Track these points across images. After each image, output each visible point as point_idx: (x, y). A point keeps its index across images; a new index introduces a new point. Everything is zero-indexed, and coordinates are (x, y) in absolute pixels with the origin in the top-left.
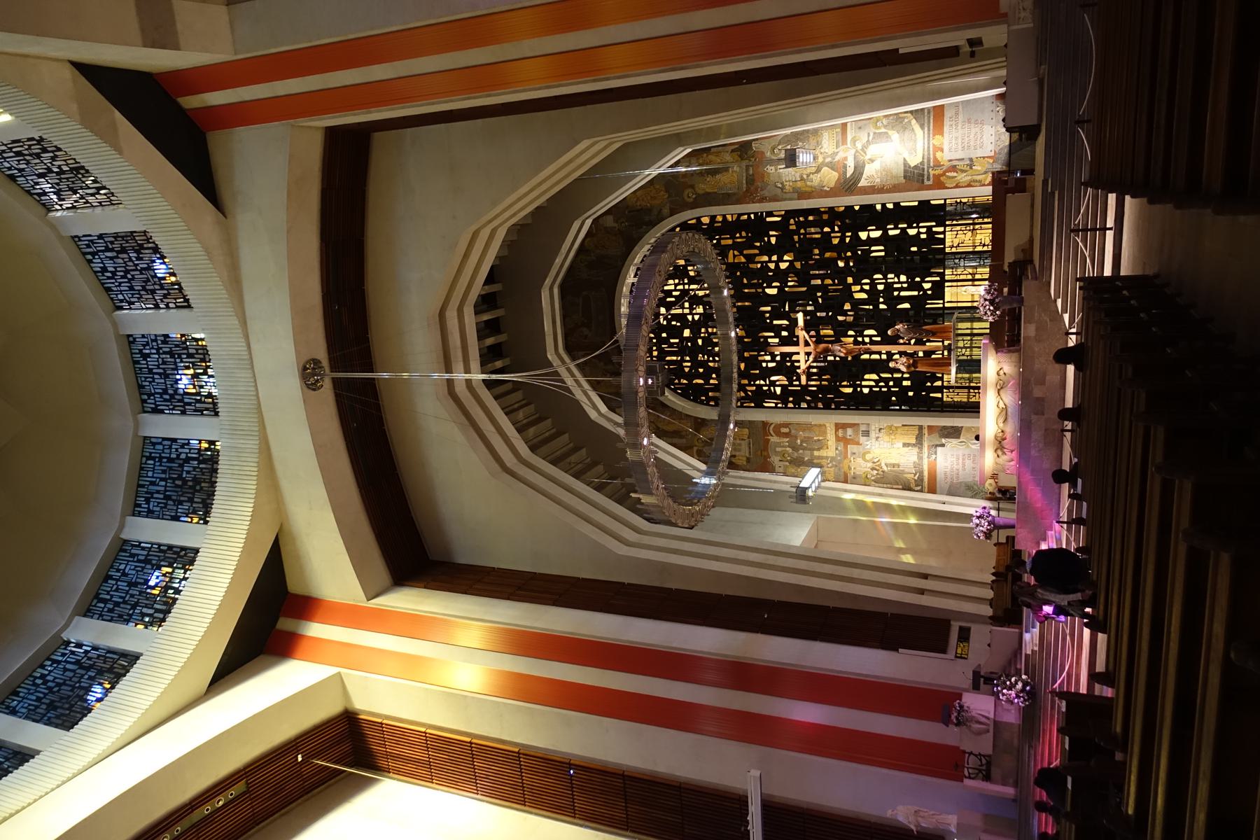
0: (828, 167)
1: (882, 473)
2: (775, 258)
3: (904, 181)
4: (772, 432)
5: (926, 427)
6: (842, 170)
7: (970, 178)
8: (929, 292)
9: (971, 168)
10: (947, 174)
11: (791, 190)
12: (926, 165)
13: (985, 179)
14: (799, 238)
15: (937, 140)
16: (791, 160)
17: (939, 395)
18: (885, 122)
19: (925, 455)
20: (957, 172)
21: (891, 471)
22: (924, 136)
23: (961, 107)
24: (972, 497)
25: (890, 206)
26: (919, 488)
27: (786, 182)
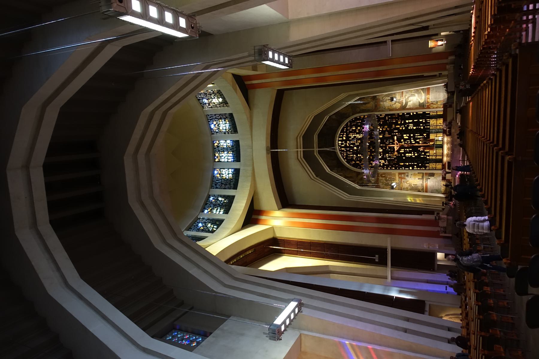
2: (382, 127)
3: (419, 107)
6: (402, 103)
7: (436, 106)
8: (426, 137)
13: (441, 106)
14: (389, 122)
15: (428, 96)
16: (392, 99)
17: (428, 165)
18: (414, 91)
19: (424, 182)
23: (434, 88)
24: (438, 193)
25: (415, 113)
26: (423, 191)
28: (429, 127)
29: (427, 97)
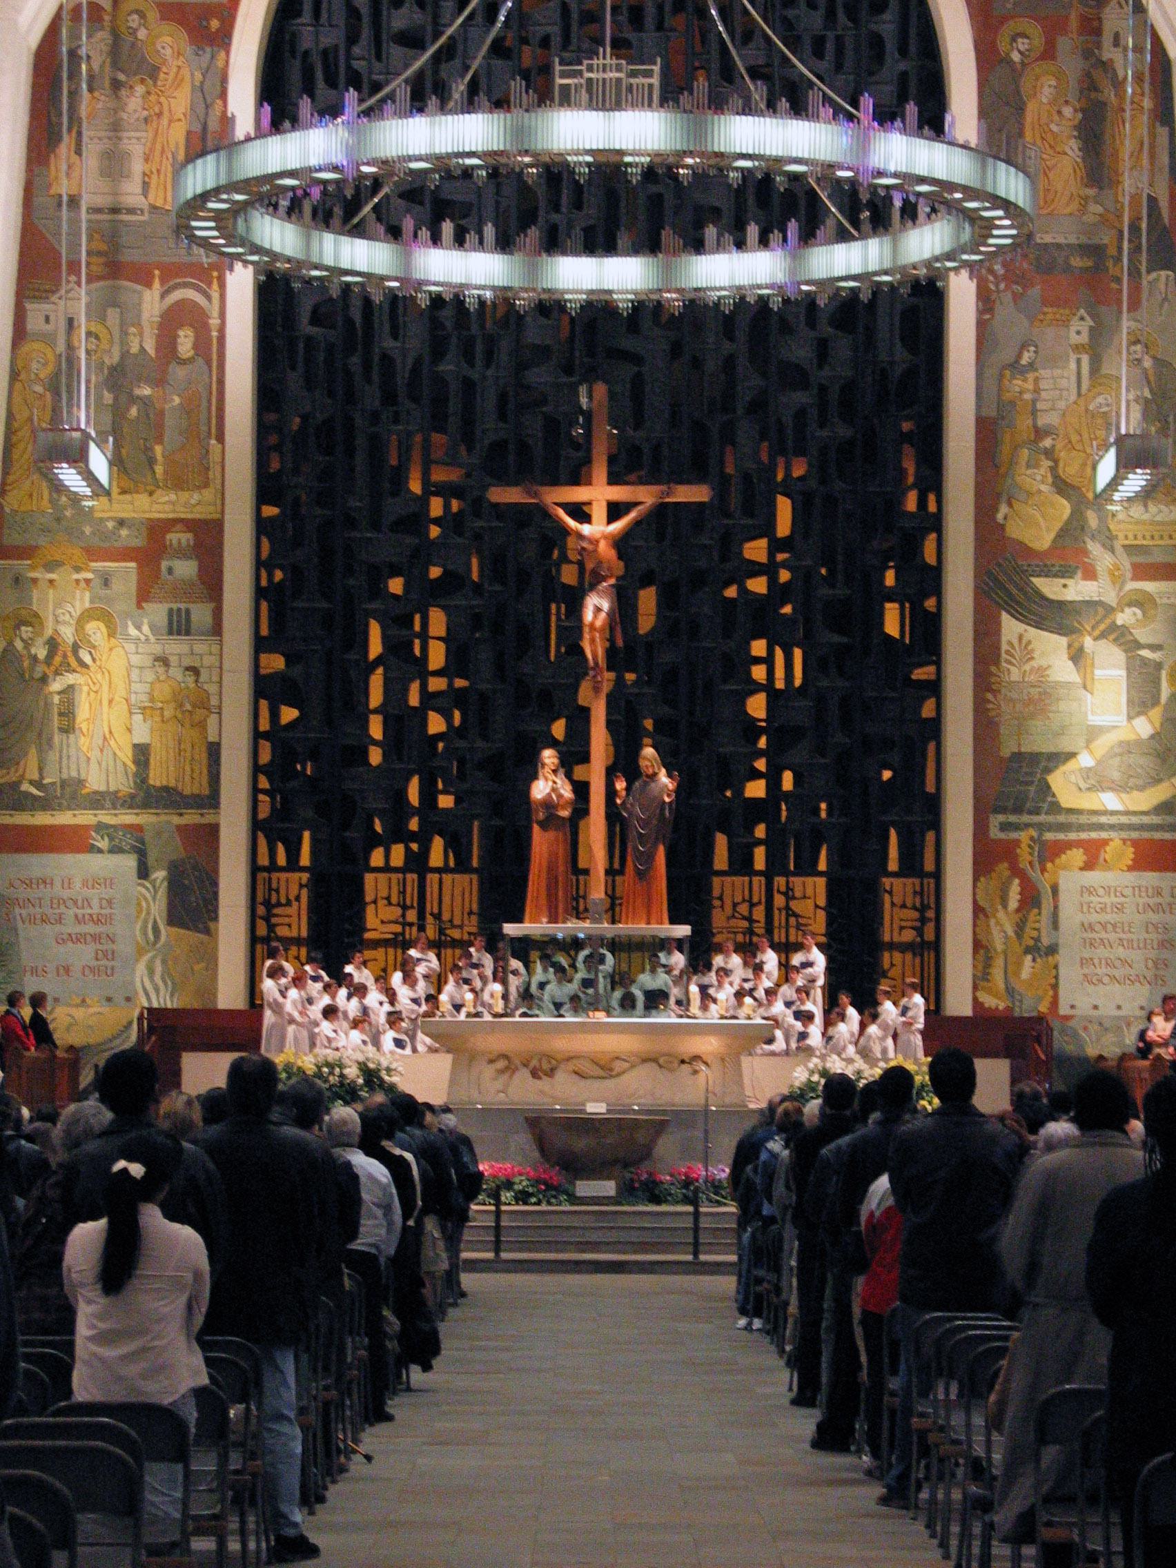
0: (1069, 521)
1: (37, 675)
3: (1006, 752)
4: (178, 295)
5: (209, 819)
7: (999, 945)
9: (1028, 951)
10: (1017, 881)
11: (1007, 396)
12: (1050, 819)
13: (989, 991)
15: (1118, 848)
19: (106, 818)
20: (1018, 910)
21: (48, 705)
22: (1135, 813)
27: (1036, 380)
28: (760, 861)
29: (1116, 844)
